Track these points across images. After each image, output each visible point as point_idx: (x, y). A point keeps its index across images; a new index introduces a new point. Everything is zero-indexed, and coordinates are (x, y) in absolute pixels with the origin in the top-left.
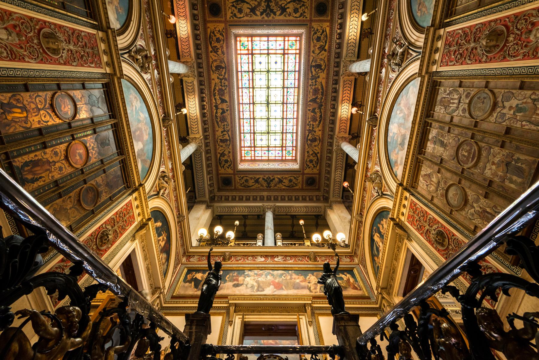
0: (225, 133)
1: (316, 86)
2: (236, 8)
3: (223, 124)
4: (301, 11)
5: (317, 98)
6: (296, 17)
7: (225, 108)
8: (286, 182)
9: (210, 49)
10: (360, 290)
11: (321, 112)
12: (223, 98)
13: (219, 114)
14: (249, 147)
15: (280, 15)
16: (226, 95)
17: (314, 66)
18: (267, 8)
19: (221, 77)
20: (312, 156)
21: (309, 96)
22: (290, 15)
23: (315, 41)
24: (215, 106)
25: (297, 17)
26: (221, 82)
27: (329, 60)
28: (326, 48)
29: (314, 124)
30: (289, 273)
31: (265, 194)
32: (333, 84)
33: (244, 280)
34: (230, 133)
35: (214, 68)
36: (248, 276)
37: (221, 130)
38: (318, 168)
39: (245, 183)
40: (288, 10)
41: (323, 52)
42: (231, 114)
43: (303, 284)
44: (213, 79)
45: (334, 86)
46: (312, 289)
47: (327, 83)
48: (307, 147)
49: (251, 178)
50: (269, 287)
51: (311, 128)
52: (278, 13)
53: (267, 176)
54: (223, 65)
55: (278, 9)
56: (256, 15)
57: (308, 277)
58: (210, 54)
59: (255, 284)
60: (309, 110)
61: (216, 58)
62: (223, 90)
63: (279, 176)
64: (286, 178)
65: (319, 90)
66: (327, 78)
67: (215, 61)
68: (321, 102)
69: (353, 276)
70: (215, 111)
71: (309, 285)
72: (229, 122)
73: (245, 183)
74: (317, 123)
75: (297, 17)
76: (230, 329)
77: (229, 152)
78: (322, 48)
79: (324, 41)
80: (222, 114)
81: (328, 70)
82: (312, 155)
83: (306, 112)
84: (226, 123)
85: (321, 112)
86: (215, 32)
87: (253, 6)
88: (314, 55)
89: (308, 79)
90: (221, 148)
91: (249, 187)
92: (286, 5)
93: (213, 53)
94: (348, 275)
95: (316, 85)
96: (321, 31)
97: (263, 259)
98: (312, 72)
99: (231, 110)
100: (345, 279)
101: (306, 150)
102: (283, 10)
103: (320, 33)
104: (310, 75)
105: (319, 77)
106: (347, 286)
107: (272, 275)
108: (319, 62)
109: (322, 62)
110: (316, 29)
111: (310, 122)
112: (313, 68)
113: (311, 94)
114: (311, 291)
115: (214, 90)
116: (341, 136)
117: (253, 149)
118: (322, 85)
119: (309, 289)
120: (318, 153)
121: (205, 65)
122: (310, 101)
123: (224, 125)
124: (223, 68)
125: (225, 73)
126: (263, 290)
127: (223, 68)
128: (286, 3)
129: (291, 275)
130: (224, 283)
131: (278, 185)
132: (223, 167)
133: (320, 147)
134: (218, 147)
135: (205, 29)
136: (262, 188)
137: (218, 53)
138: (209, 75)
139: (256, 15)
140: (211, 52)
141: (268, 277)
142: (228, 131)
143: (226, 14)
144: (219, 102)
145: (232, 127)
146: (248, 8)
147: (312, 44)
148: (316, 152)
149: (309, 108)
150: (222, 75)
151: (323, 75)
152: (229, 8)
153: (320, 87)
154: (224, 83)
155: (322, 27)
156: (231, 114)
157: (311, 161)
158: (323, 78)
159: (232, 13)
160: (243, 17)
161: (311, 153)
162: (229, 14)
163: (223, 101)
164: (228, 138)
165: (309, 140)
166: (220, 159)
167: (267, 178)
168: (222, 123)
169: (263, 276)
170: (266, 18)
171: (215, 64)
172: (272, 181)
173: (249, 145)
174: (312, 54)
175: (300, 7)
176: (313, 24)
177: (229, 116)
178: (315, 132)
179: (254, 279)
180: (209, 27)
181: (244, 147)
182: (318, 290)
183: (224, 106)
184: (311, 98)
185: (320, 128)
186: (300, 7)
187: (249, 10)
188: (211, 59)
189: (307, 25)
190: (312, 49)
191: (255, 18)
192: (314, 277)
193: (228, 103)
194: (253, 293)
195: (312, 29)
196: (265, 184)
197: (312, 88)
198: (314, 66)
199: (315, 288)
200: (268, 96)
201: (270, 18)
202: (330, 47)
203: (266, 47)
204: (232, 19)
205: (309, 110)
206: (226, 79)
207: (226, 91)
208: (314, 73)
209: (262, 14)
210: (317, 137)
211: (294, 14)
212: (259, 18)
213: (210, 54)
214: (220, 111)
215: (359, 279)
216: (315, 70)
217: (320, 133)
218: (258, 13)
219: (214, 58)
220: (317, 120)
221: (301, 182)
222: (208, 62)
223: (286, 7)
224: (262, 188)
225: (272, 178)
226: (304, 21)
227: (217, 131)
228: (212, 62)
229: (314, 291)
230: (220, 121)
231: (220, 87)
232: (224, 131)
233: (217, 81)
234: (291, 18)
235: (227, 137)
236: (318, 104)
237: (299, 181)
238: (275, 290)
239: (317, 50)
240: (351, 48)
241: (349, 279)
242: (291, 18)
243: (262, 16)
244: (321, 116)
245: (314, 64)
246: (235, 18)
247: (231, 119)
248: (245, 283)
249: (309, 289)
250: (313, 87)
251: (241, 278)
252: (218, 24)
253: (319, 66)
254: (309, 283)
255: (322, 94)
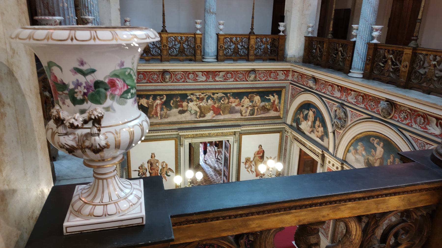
10: (279, 111)
30: (227, 96)
33: (188, 106)
36: (192, 101)
43: (238, 108)
46: (243, 113)
50: (209, 112)
57: (243, 100)
59: (198, 110)
69: (280, 98)
71: (242, 108)
76: (182, 149)
94: (276, 96)
97: (204, 78)
100: (272, 101)
106: (271, 109)
107: (213, 99)
114: (242, 115)
119: (241, 113)
126: (204, 116)
129: (229, 99)
130: (170, 110)
141: (209, 101)
169: (205, 101)
179: (197, 105)
182: (248, 114)
192: (248, 100)
194: (196, 119)
199: (246, 112)
215: (282, 101)
229: (244, 115)
238: (214, 115)
241: (274, 101)
248: (189, 109)
249: (241, 113)
251: (185, 104)
254: (243, 106)
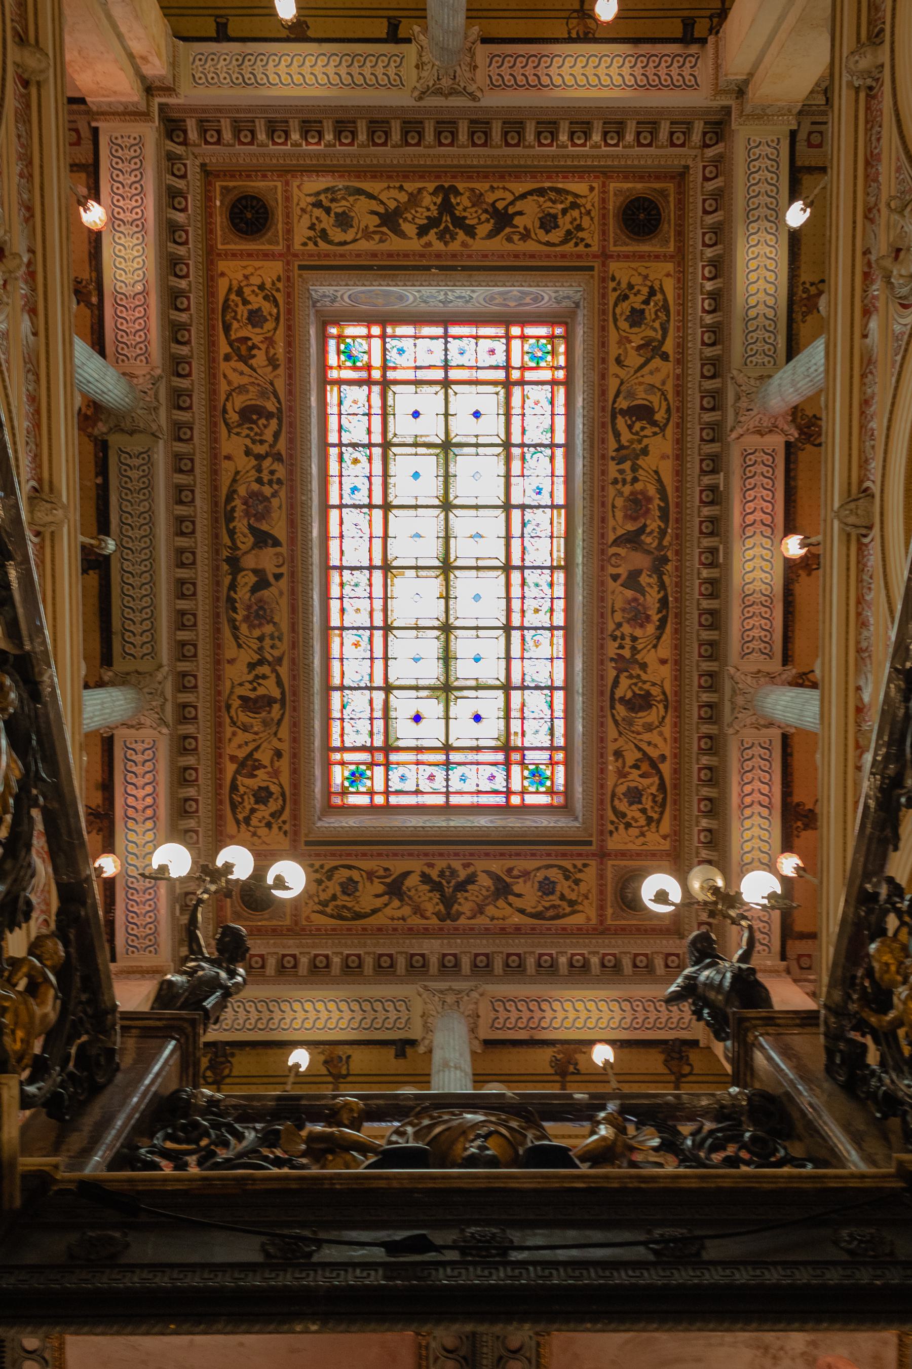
0: (265, 669)
1: (639, 486)
2: (328, 211)
3: (257, 633)
4: (565, 223)
5: (642, 530)
6: (548, 244)
7: (270, 568)
8: (528, 894)
9: (224, 348)
11: (662, 586)
12: (264, 527)
13: (243, 594)
14: (363, 749)
15: (491, 235)
16: (275, 515)
17: (623, 413)
18: (441, 214)
19: (261, 449)
20: (636, 772)
21: (611, 523)
22: (526, 236)
23: (624, 325)
24: (228, 560)
25: (554, 245)
26: (259, 470)
27: (680, 391)
28: (669, 346)
29: (638, 632)
31: (432, 948)
32: (703, 472)
34: (284, 671)
35: (233, 417)
37: (247, 656)
38: (666, 826)
39: (343, 900)
40: (517, 220)
41: (657, 362)
42: (293, 592)
44: (228, 458)
45: (707, 480)
47: (679, 473)
48: (612, 732)
49: (370, 875)
51: (626, 653)
52: (483, 230)
53: (441, 864)
54: (271, 406)
55: (484, 217)
56: (402, 235)
58: (224, 366)
60: (615, 578)
61: (245, 380)
62: (267, 499)
63: (496, 866)
64: (526, 874)
65: (649, 500)
66: (680, 457)
67: (242, 389)
68: (660, 547)
70: (227, 580)
72: (285, 626)
73: (343, 900)
74: (651, 629)
75: (554, 245)
77: (278, 754)
78: (652, 349)
79: (657, 325)
80: (255, 589)
81: (681, 426)
82: (636, 767)
83: (602, 583)
84: (268, 629)
85: (662, 586)
86: (247, 291)
87: (392, 205)
88: (622, 373)
89: (603, 457)
90: (242, 737)
91: (358, 916)
92: (512, 203)
93: (233, 363)
95: (635, 480)
96: (645, 291)
98: (617, 435)
99: (293, 574)
101: (611, 747)
102: (502, 219)
103: (641, 298)
104: (612, 444)
105: (645, 452)
108: (642, 397)
109: (655, 400)
110: (624, 285)
111: (619, 625)
112: (621, 422)
113: (619, 515)
115: (230, 498)
116: (754, 669)
117: (379, 757)
118: (659, 481)
120: (663, 758)
121: (199, 401)
122: (616, 542)
123: (261, 639)
124: (270, 415)
125: (276, 435)
127: (270, 415)
128: (510, 198)
131: (490, 910)
132: (247, 821)
133: (667, 730)
134: (229, 730)
135: (210, 278)
136: (416, 921)
137: (253, 362)
138: (214, 440)
139: (402, 235)
140: (227, 358)
142: (279, 660)
143: (289, 231)
144: (246, 541)
145: (294, 645)
146: (374, 213)
147: (613, 336)
148: (654, 753)
149: (612, 570)
150: (262, 442)
151: (660, 447)
152: (303, 210)
153: (652, 491)
154: (272, 472)
155: (646, 277)
156: (293, 592)
157: (635, 796)
158: (664, 457)
159: (312, 227)
160: (355, 241)
161: (631, 756)
162: (301, 231)
163: (263, 539)
164: (276, 693)
165: (622, 699)
166: (234, 787)
167: (442, 874)
168: (252, 627)
170: (438, 246)
171: (239, 401)
172: (461, 887)
173: (363, 739)
174: (613, 368)
175: (564, 212)
176: (614, 267)
177: (284, 602)
178: (644, 666)
180: (223, 274)
181: (343, 749)
183: (267, 559)
184: (620, 532)
185: (665, 650)
186: (564, 212)
187: (376, 220)
188: (223, 382)
189: (591, 268)
190: (614, 351)
191: (395, 244)
193: (283, 550)
195: (612, 285)
196: (432, 904)
197: (620, 493)
198: (623, 413)
200: (447, 538)
201: (455, 246)
202: (681, 346)
203: (438, 359)
204: (311, 246)
205: (615, 578)
206: (278, 458)
207: (275, 502)
208: (626, 436)
209: (422, 231)
210: (655, 691)
211: (541, 233)
212: (414, 244)
213: (224, 366)
214: (247, 580)
216: (630, 427)
217: (666, 672)
218: (410, 229)
219: (237, 380)
220: (648, 618)
221: (593, 896)
222: (213, 393)
223: (511, 210)
224: (416, 921)
225: (463, 874)
226: (579, 256)
227: (231, 662)
228: (229, 395)
230: (246, 619)
231: (255, 487)
232: (261, 662)
233: (245, 464)
234: (531, 246)
235: (270, 688)
236: (649, 552)
237: (583, 888)
239: (632, 353)
240: (760, 334)
242: (531, 246)
243: (425, 239)
244: (664, 602)
245: (623, 404)
246: (323, 245)
247: (293, 610)
250: (627, 490)
252: (258, 264)
253: (644, 413)
255: (664, 515)
